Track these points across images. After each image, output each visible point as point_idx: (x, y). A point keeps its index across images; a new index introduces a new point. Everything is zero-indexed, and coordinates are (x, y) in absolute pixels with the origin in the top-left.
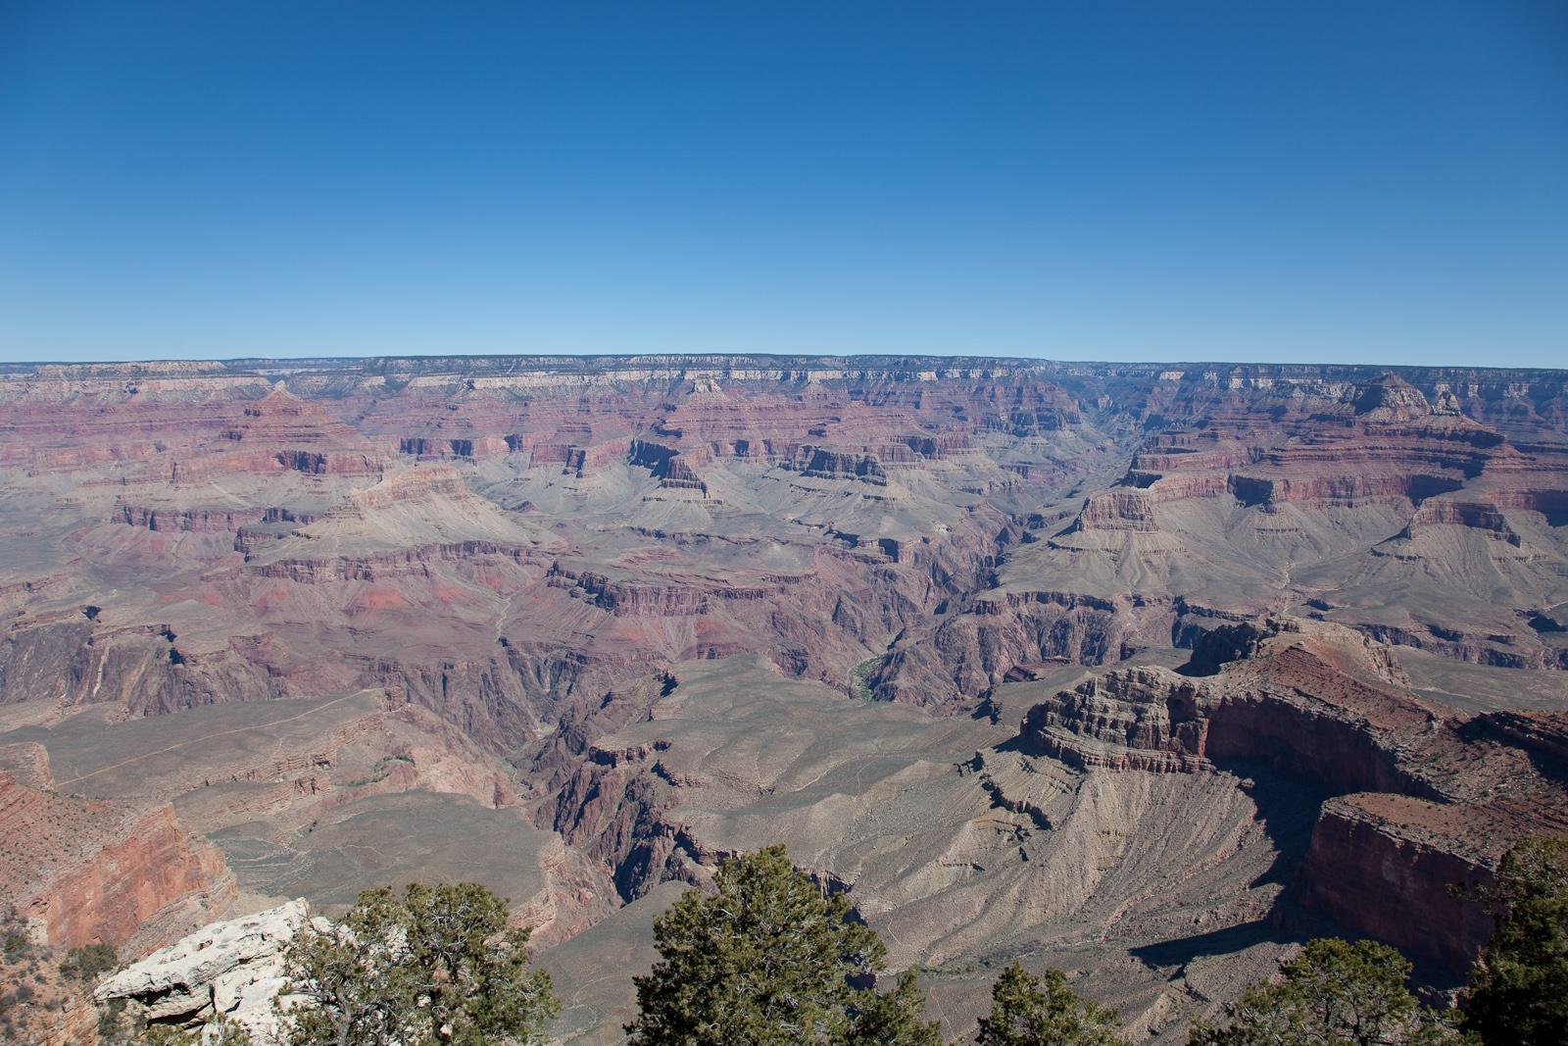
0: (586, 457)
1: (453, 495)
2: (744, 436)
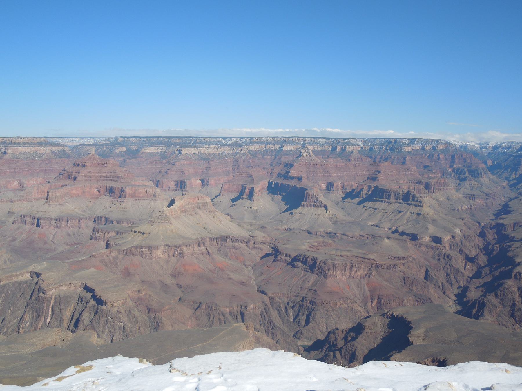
0: (255, 190)
1: (208, 211)
2: (331, 180)
